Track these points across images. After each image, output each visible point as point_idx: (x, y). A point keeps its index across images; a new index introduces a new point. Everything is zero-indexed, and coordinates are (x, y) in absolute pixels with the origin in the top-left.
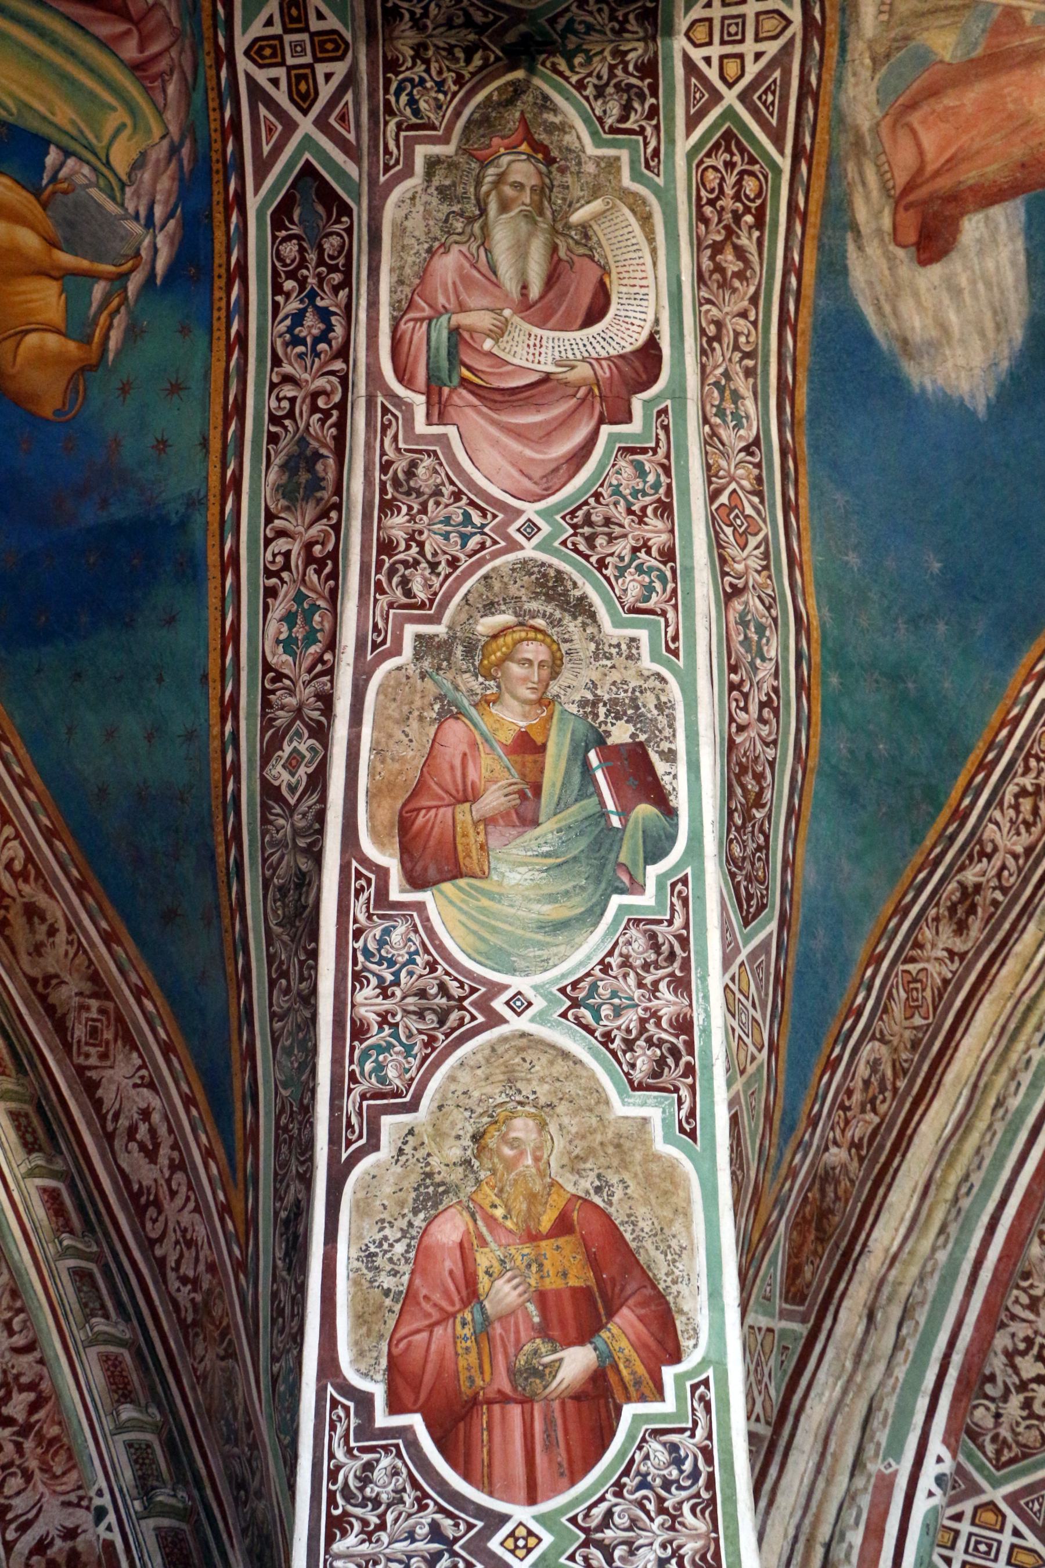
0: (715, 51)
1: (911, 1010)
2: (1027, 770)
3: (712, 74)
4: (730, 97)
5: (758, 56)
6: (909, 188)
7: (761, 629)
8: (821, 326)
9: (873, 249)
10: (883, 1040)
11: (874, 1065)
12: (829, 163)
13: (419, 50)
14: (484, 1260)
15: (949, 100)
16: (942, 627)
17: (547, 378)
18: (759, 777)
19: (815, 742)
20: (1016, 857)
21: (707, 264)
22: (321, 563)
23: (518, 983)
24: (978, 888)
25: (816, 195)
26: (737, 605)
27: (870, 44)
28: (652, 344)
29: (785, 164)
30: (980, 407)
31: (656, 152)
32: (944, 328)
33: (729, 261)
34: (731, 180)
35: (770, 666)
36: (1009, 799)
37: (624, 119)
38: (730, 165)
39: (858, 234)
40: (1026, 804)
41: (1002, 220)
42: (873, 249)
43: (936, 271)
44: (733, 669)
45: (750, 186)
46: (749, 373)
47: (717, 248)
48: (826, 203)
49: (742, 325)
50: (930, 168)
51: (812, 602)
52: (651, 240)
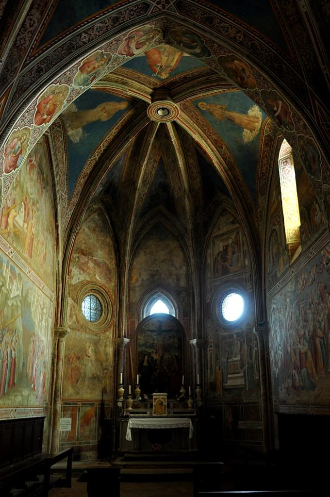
13: (164, 22)
14: (50, 102)
17: (130, 47)
22: (107, 29)
23: (73, 84)
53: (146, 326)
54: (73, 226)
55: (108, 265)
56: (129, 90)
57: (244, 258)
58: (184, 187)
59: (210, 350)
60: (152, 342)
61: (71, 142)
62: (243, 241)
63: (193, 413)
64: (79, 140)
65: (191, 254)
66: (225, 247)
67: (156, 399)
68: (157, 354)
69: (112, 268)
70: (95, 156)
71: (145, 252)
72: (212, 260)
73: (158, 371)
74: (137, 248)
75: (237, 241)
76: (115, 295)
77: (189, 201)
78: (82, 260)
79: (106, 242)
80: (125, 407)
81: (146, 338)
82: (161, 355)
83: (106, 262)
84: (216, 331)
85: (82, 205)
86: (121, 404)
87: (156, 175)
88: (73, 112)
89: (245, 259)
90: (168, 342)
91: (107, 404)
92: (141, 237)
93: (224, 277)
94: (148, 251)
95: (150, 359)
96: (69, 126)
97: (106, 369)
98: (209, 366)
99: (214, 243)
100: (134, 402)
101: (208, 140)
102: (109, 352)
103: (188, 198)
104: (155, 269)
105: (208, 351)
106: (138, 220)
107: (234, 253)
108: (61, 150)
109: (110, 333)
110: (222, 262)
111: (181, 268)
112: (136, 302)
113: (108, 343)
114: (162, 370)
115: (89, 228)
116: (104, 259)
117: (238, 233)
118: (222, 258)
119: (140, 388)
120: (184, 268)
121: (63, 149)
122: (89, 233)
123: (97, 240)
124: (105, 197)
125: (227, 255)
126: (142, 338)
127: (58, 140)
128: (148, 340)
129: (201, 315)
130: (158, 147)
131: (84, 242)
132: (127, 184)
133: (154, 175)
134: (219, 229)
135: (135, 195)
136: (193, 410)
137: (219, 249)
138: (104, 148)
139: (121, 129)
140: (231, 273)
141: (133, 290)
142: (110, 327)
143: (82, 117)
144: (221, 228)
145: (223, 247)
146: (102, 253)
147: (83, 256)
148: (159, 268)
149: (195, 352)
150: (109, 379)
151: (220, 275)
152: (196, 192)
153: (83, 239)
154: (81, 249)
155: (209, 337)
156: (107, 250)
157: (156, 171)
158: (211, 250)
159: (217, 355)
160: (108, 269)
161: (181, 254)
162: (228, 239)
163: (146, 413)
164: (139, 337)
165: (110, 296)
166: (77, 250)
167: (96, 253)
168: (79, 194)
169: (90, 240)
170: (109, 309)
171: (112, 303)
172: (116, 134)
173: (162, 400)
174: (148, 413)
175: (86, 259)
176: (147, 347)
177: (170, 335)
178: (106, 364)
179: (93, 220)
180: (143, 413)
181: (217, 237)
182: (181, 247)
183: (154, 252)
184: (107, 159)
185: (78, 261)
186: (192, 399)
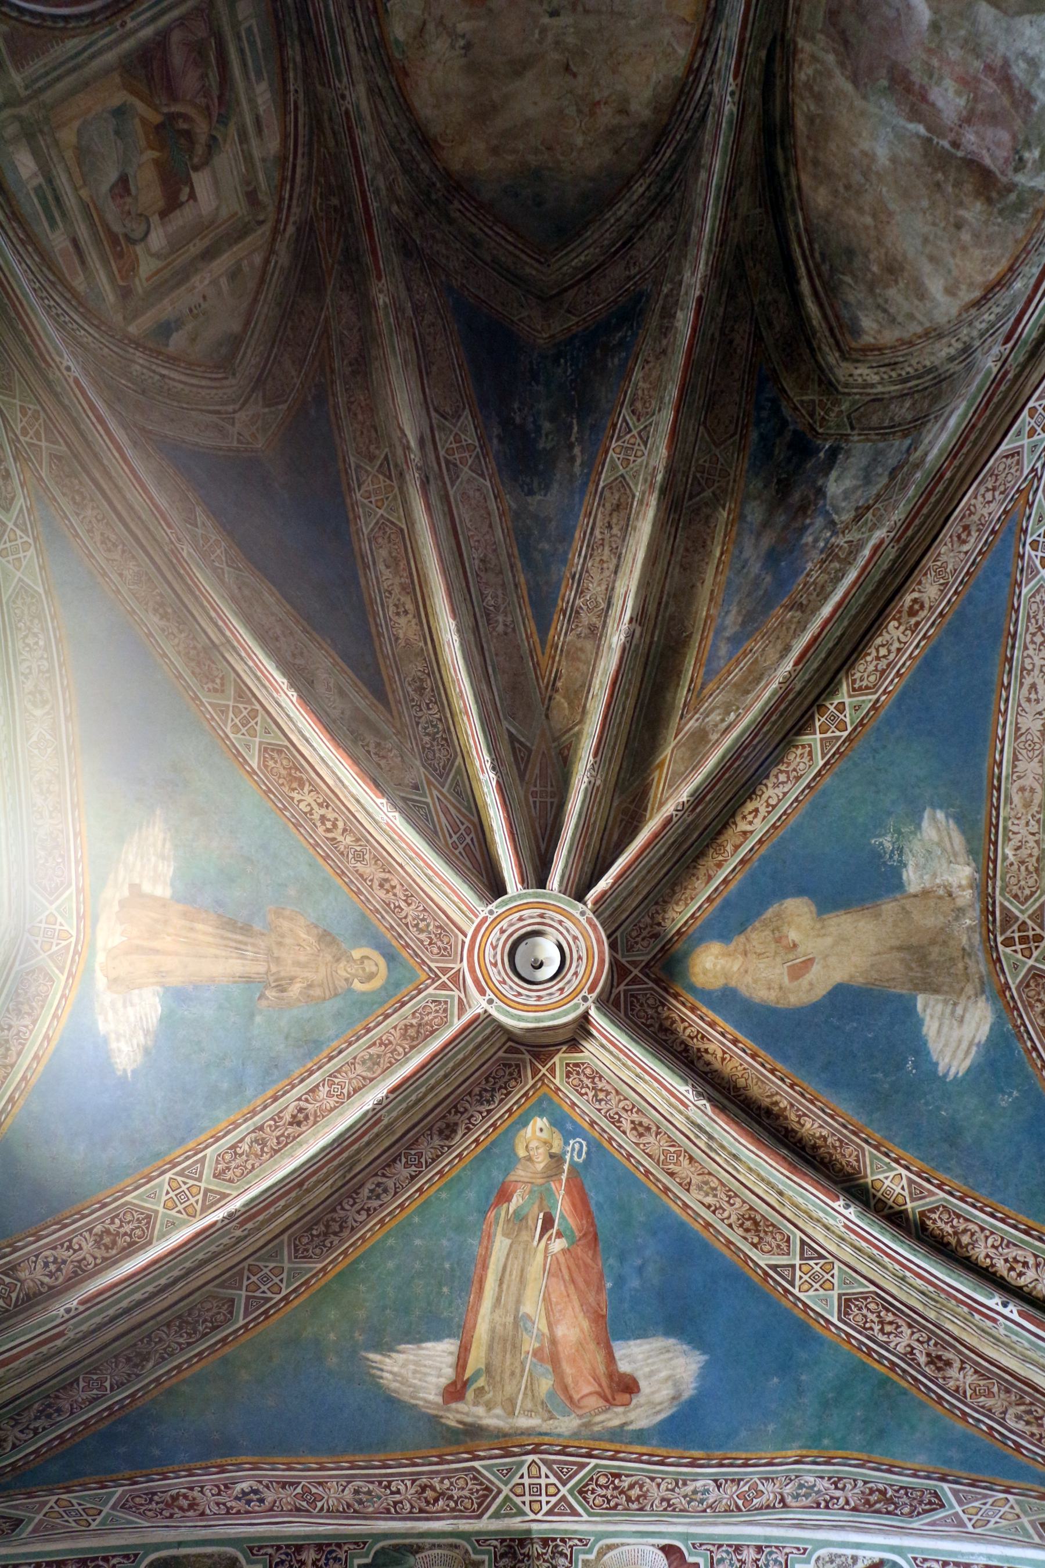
0: (544, 1498)
1: (990, 1394)
2: (871, 1329)
3: (554, 1500)
4: (564, 1491)
5: (547, 1477)
6: (607, 1400)
7: (801, 1486)
8: (664, 1443)
9: (632, 1416)
10: (1005, 1412)
11: (1019, 1418)
12: (594, 1439)
15: (569, 1380)
16: (803, 1377)
18: (872, 1492)
19: (856, 1455)
20: (913, 1333)
21: (635, 1506)
24: (928, 1355)
25: (608, 1446)
26: (789, 1500)
27: (544, 1421)
28: (664, 1549)
29: (594, 1462)
30: (705, 1358)
31: (580, 1540)
32: (668, 1378)
33: (634, 1493)
34: (599, 1491)
35: (818, 1481)
36: (885, 1338)
37: (566, 1556)
38: (593, 1491)
39: (625, 1424)
40: (888, 1328)
41: (623, 1352)
42: (632, 1416)
43: (643, 1384)
44: (818, 1505)
45: (602, 1481)
46: (685, 1484)
47: (629, 1499)
48: (612, 1441)
49: (663, 1486)
50: (598, 1389)
51: (789, 1453)
52: (617, 1546)
54: (1017, 377)
55: (842, 64)
56: (686, 1106)
57: (50, 181)
58: (428, 507)
61: (963, 821)
62: (83, 262)
64: (925, 824)
65: (366, 138)
66: (184, 197)
69: (819, 37)
70: (857, 708)
71: (623, 111)
72: (245, 105)
74: (661, 136)
75: (120, 255)
77: (402, 431)
78: (998, 144)
79: (835, 193)
83: (848, 87)
85: (951, 480)
87: (566, 536)
88: (936, 991)
89: (40, 180)
92: (639, 188)
93: (148, 32)
94: (607, 117)
96: (960, 911)
99: (252, 197)
101: (330, 782)
103: (407, 448)
104: (566, 19)
106: (658, 283)
107: (123, 187)
108: (1016, 799)
110: (180, 115)
111: (422, 30)
115: (921, 293)
116: (859, 103)
117: (125, 294)
118: (188, 135)
120: (398, 31)
121: (1009, 800)
122: (927, 268)
123: (881, 213)
124: (812, 416)
125: (156, 162)
127: (1024, 853)
130: (558, 697)
131: (966, 236)
132: (708, 493)
133: (577, 535)
134: (234, 274)
135: (671, 458)
137: (216, 182)
138: (806, 739)
139: (725, 826)
140: (107, 71)
143: (900, 949)
144: (223, 281)
145: (192, 196)
146: (865, 145)
147: (988, 161)
148: (544, 31)
151: (176, 36)
152: (372, 458)
153: (964, 249)
154: (989, 201)
156: (832, 146)
157: (564, 561)
158: (257, 154)
160: (846, 43)
161: (424, 105)
162: (175, 246)
166: (1020, 206)
167: (905, 154)
168: (953, 527)
169: (926, 229)
172: (750, 806)
175: (970, 137)
179: (893, 320)
181: (241, 232)
182: (427, 143)
183: (571, 111)
184: (799, 693)
185: (1028, 145)
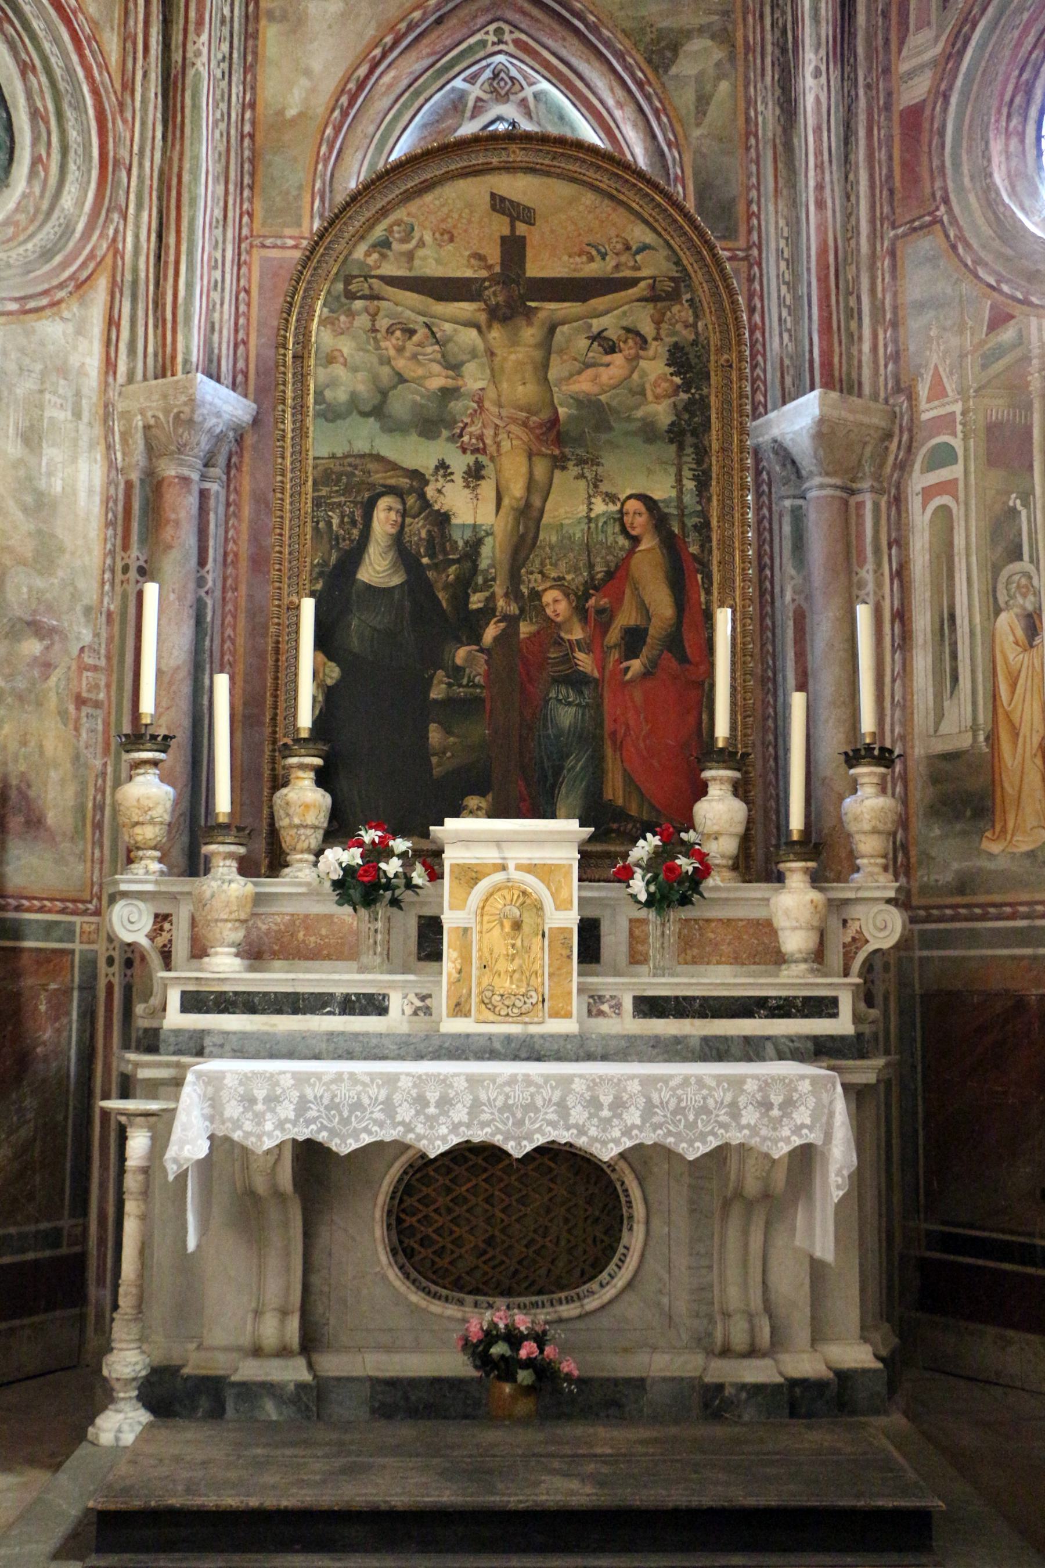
53: (384, 244)
59: (928, 494)
60: (436, 383)
63: (824, 1007)
67: (471, 875)
68: (487, 489)
73: (490, 633)
76: (127, 38)
80: (181, 949)
81: (389, 346)
82: (517, 489)
84: (999, 320)
86: (147, 923)
90: (583, 385)
91: (50, 926)
95: (419, 529)
97: (36, 628)
98: (922, 622)
100: (259, 899)
102: (70, 490)
105: (915, 503)
109: (80, 331)
112: (301, 115)
113: (63, 416)
114: (525, 629)
119: (323, 779)
126: (346, 347)
128: (401, 364)
129: (849, 214)
136: (820, 986)
141: (284, 18)
142: (81, 285)
149: (798, 517)
150: (63, 714)
155: (923, 390)
159: (1013, 512)
163: (374, 1005)
164: (321, 336)
165: (84, 29)
170: (73, 135)
171: (95, 92)
173: (533, 883)
174: (395, 1003)
176: (393, 427)
177: (597, 325)
178: (39, 583)
180: (350, 1005)
186: (816, 879)
